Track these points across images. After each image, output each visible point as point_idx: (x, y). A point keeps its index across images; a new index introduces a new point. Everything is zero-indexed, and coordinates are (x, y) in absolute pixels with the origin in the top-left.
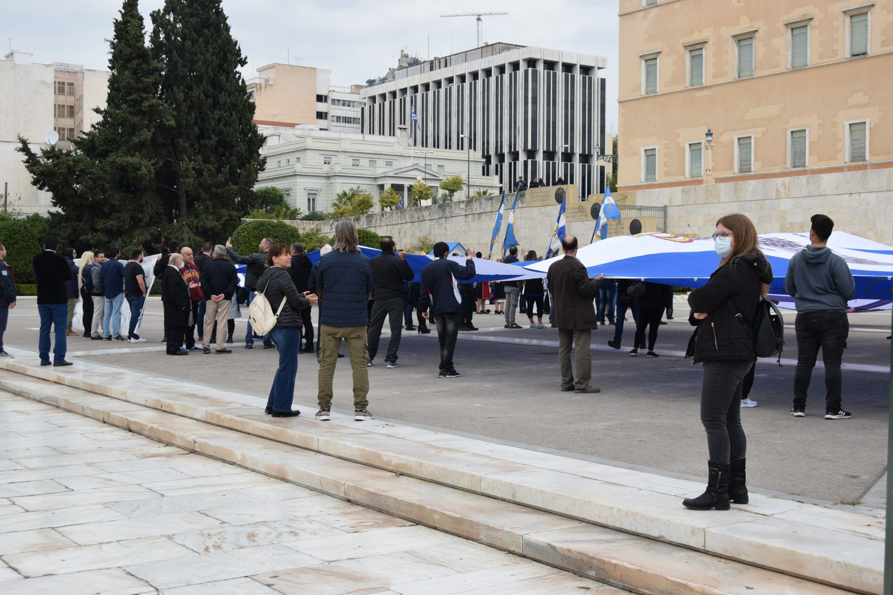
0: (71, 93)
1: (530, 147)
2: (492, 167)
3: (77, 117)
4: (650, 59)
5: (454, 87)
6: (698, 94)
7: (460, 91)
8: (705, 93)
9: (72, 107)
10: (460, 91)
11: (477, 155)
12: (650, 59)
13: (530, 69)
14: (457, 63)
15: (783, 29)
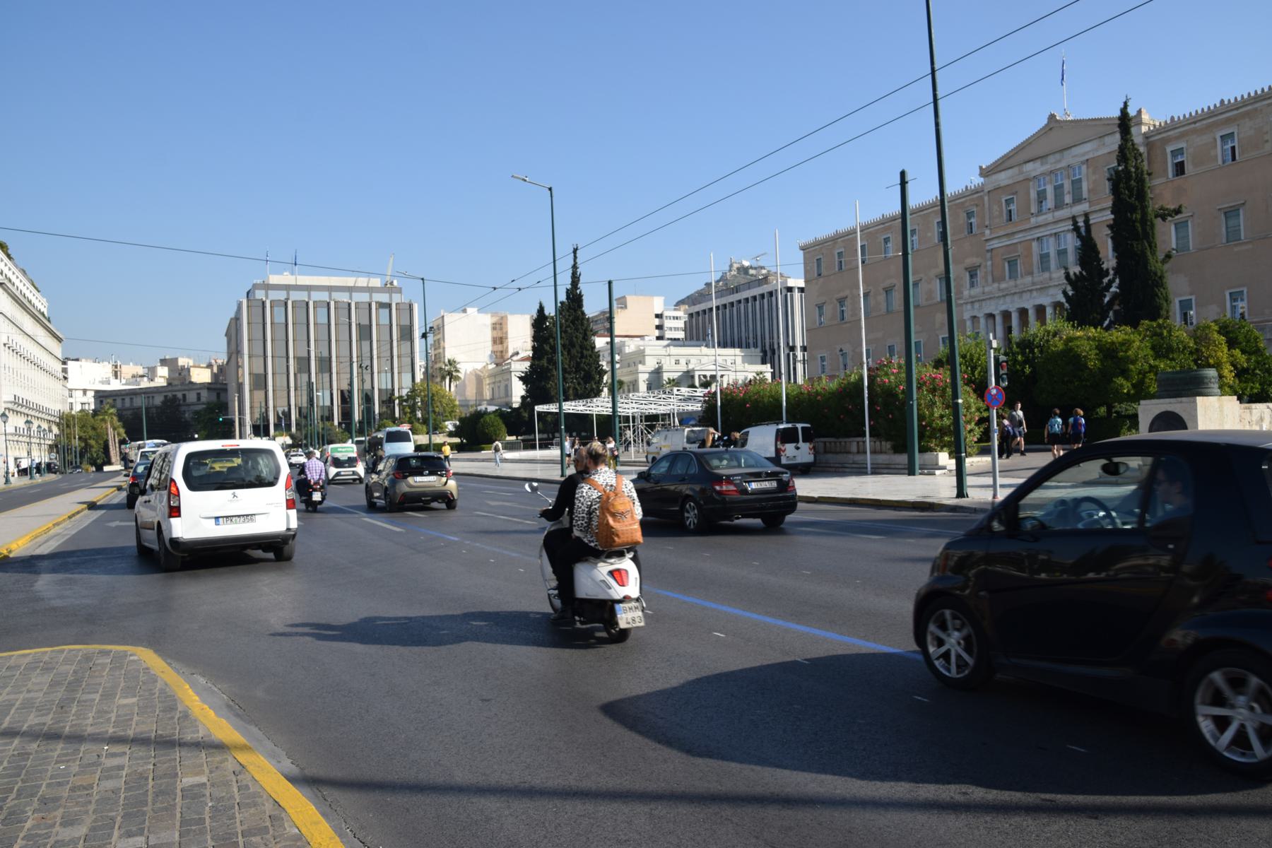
0: (501, 329)
1: (791, 344)
2: (768, 358)
3: (505, 345)
4: (820, 307)
5: (742, 306)
6: (845, 326)
7: (746, 309)
8: (848, 325)
9: (501, 338)
10: (746, 309)
11: (759, 350)
12: (820, 307)
13: (789, 294)
14: (744, 290)
15: (882, 291)
